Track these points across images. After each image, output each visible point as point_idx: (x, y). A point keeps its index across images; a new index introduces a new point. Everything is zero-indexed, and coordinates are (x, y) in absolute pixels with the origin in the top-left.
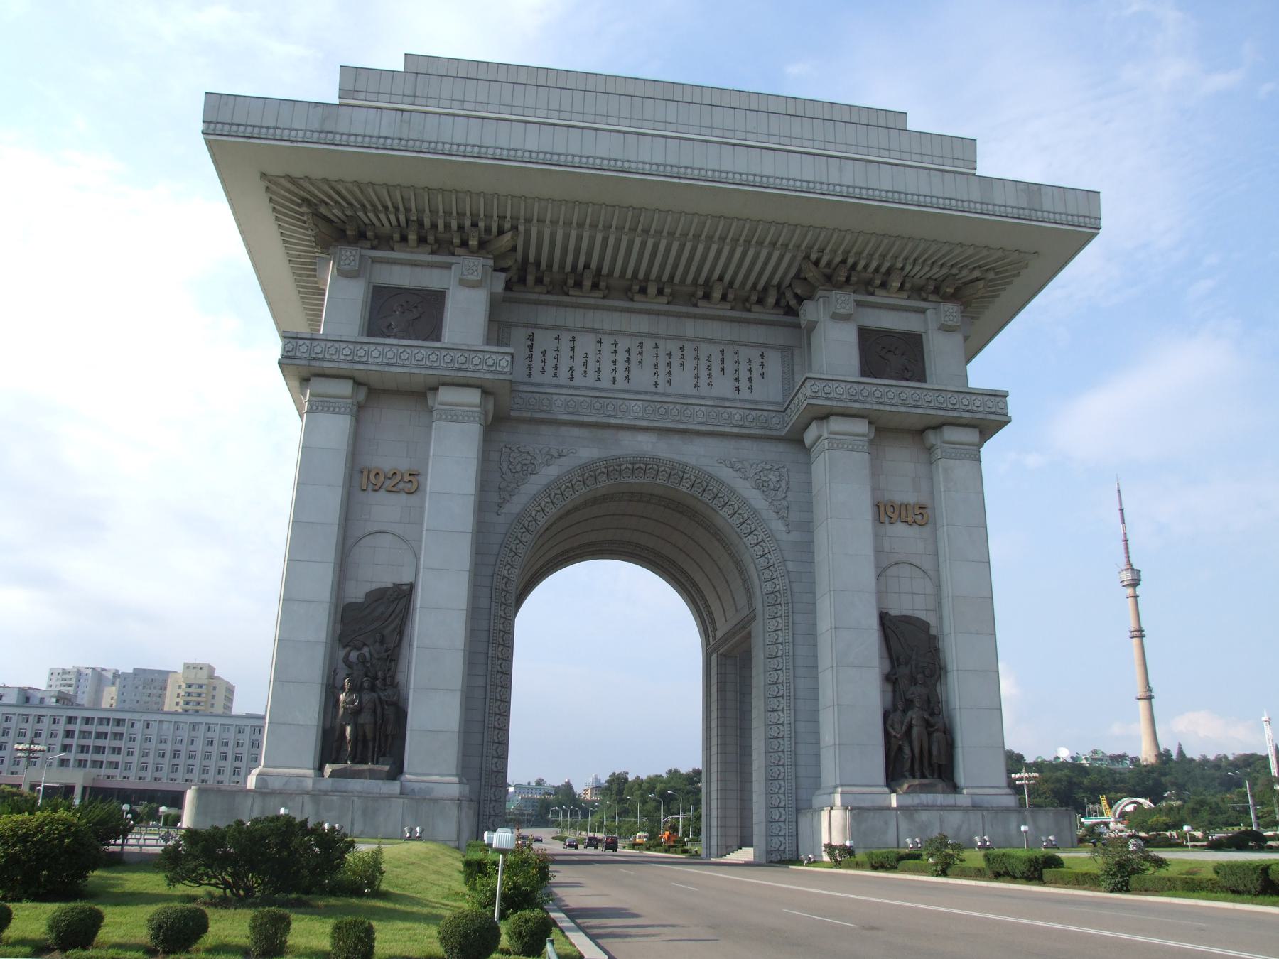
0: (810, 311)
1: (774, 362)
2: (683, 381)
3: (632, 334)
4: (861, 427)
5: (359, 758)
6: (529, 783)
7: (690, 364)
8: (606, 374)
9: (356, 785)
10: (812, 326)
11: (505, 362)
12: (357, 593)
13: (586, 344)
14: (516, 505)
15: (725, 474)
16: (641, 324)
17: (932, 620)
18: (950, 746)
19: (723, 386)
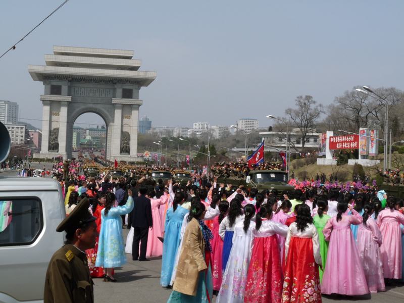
0: (116, 86)
1: (111, 91)
2: (97, 94)
3: (90, 88)
4: (121, 105)
5: (53, 150)
6: (98, 127)
7: (98, 92)
8: (86, 95)
9: (53, 153)
10: (116, 89)
11: (70, 99)
12: (52, 129)
13: (83, 89)
14: (73, 115)
15: (103, 110)
16: (91, 86)
17: (129, 132)
18: (129, 149)
19: (103, 95)
